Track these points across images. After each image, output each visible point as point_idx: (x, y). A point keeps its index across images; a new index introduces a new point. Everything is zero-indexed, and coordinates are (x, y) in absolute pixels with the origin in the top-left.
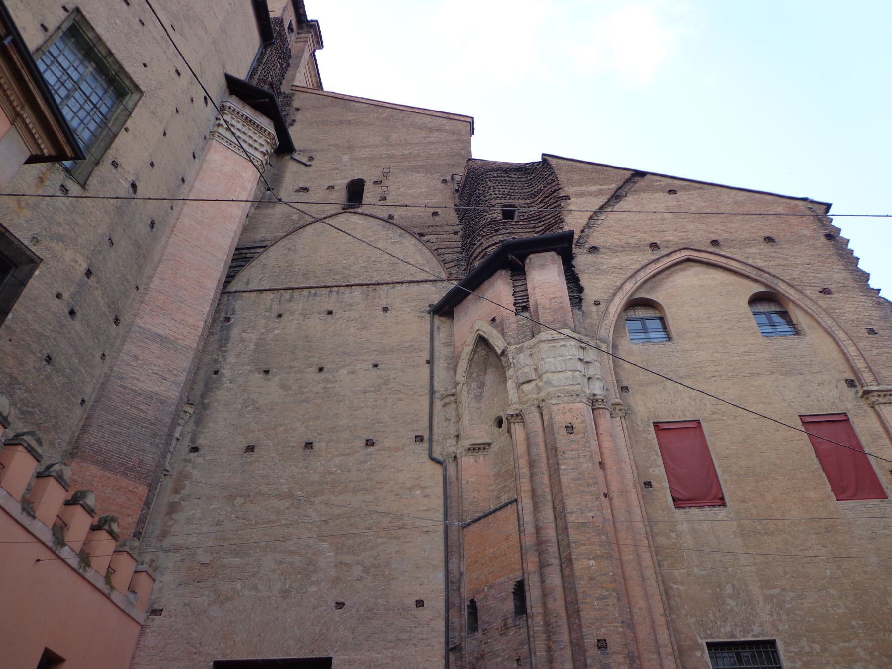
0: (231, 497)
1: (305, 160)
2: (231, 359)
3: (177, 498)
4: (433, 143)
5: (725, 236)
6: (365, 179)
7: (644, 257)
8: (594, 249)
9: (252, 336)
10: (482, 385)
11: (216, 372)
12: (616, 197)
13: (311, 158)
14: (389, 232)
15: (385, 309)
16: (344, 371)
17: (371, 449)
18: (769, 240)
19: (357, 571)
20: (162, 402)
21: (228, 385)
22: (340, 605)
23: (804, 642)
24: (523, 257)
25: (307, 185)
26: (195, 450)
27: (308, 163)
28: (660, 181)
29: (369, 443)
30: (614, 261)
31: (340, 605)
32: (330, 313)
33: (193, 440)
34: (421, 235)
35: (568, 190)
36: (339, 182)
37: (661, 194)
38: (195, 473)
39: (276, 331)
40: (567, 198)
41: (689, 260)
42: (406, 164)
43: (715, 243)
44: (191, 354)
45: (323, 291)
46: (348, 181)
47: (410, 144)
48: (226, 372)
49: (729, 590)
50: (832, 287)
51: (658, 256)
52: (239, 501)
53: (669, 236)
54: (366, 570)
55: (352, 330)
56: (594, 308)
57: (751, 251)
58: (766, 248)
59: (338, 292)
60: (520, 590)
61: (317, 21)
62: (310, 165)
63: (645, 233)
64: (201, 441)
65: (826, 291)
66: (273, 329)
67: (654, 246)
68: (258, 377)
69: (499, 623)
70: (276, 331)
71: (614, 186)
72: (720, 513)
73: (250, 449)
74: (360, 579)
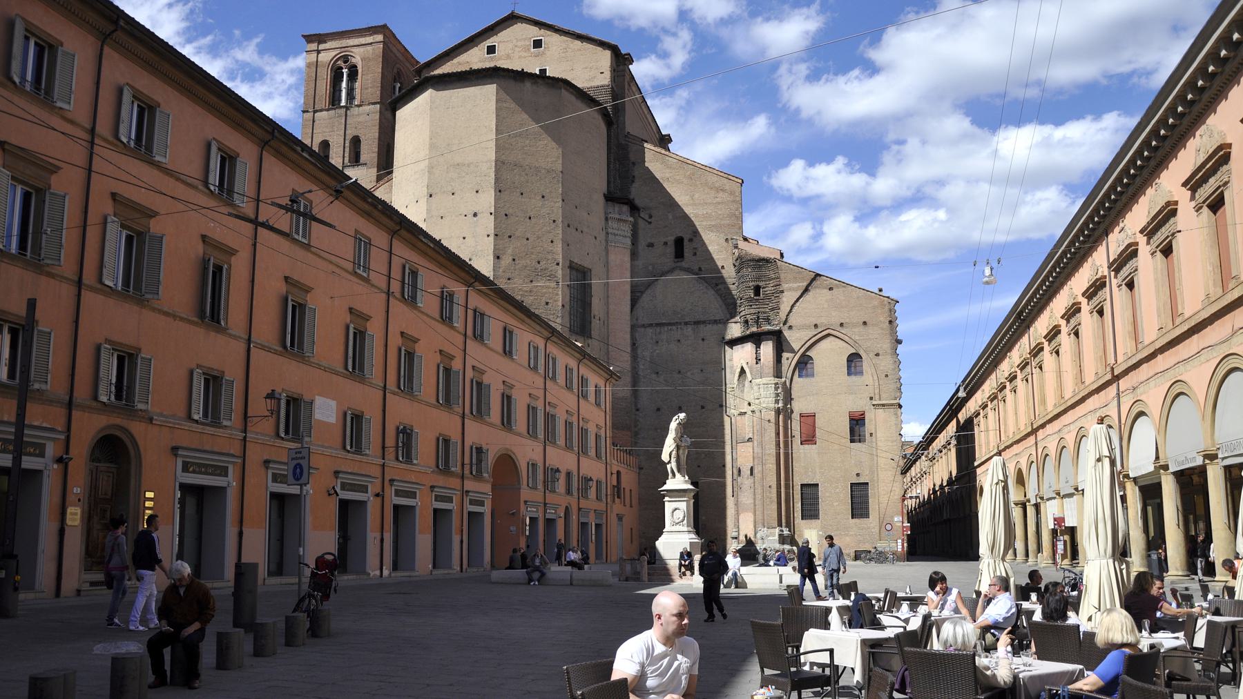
0: (656, 429)
1: (647, 217)
2: (642, 367)
3: (636, 429)
4: (719, 203)
5: (847, 321)
6: (683, 236)
7: (810, 333)
8: (790, 327)
9: (647, 354)
10: (744, 386)
11: (637, 374)
12: (806, 290)
13: (651, 217)
14: (701, 285)
15: (703, 340)
16: (689, 374)
17: (704, 410)
18: (865, 323)
19: (703, 455)
20: (626, 399)
21: (642, 380)
22: (699, 466)
23: (826, 484)
24: (760, 336)
25: (652, 241)
26: (638, 410)
27: (649, 220)
28: (827, 280)
29: (703, 407)
30: (798, 335)
31: (699, 466)
32: (679, 341)
33: (636, 406)
34: (717, 285)
35: (785, 286)
36: (669, 238)
37: (826, 290)
38: (641, 420)
39: (657, 351)
40: (782, 292)
41: (829, 335)
42: (704, 223)
43: (842, 325)
44: (630, 374)
45: (674, 327)
46: (675, 236)
47: (706, 203)
48: (641, 373)
49: (810, 470)
50: (880, 353)
51: (816, 333)
52: (659, 431)
53: (822, 321)
54: (706, 455)
55: (690, 351)
56: (786, 361)
57: (856, 330)
58: (862, 329)
59: (681, 328)
60: (752, 469)
61: (629, 54)
62: (650, 223)
63: (814, 317)
64: (639, 406)
65: (877, 355)
66: (656, 350)
67: (816, 326)
68: (654, 376)
69: (746, 476)
70: (657, 351)
71: (805, 284)
72: (814, 446)
73: (658, 409)
74: (704, 458)
